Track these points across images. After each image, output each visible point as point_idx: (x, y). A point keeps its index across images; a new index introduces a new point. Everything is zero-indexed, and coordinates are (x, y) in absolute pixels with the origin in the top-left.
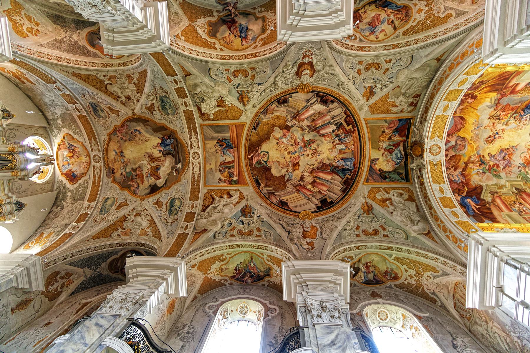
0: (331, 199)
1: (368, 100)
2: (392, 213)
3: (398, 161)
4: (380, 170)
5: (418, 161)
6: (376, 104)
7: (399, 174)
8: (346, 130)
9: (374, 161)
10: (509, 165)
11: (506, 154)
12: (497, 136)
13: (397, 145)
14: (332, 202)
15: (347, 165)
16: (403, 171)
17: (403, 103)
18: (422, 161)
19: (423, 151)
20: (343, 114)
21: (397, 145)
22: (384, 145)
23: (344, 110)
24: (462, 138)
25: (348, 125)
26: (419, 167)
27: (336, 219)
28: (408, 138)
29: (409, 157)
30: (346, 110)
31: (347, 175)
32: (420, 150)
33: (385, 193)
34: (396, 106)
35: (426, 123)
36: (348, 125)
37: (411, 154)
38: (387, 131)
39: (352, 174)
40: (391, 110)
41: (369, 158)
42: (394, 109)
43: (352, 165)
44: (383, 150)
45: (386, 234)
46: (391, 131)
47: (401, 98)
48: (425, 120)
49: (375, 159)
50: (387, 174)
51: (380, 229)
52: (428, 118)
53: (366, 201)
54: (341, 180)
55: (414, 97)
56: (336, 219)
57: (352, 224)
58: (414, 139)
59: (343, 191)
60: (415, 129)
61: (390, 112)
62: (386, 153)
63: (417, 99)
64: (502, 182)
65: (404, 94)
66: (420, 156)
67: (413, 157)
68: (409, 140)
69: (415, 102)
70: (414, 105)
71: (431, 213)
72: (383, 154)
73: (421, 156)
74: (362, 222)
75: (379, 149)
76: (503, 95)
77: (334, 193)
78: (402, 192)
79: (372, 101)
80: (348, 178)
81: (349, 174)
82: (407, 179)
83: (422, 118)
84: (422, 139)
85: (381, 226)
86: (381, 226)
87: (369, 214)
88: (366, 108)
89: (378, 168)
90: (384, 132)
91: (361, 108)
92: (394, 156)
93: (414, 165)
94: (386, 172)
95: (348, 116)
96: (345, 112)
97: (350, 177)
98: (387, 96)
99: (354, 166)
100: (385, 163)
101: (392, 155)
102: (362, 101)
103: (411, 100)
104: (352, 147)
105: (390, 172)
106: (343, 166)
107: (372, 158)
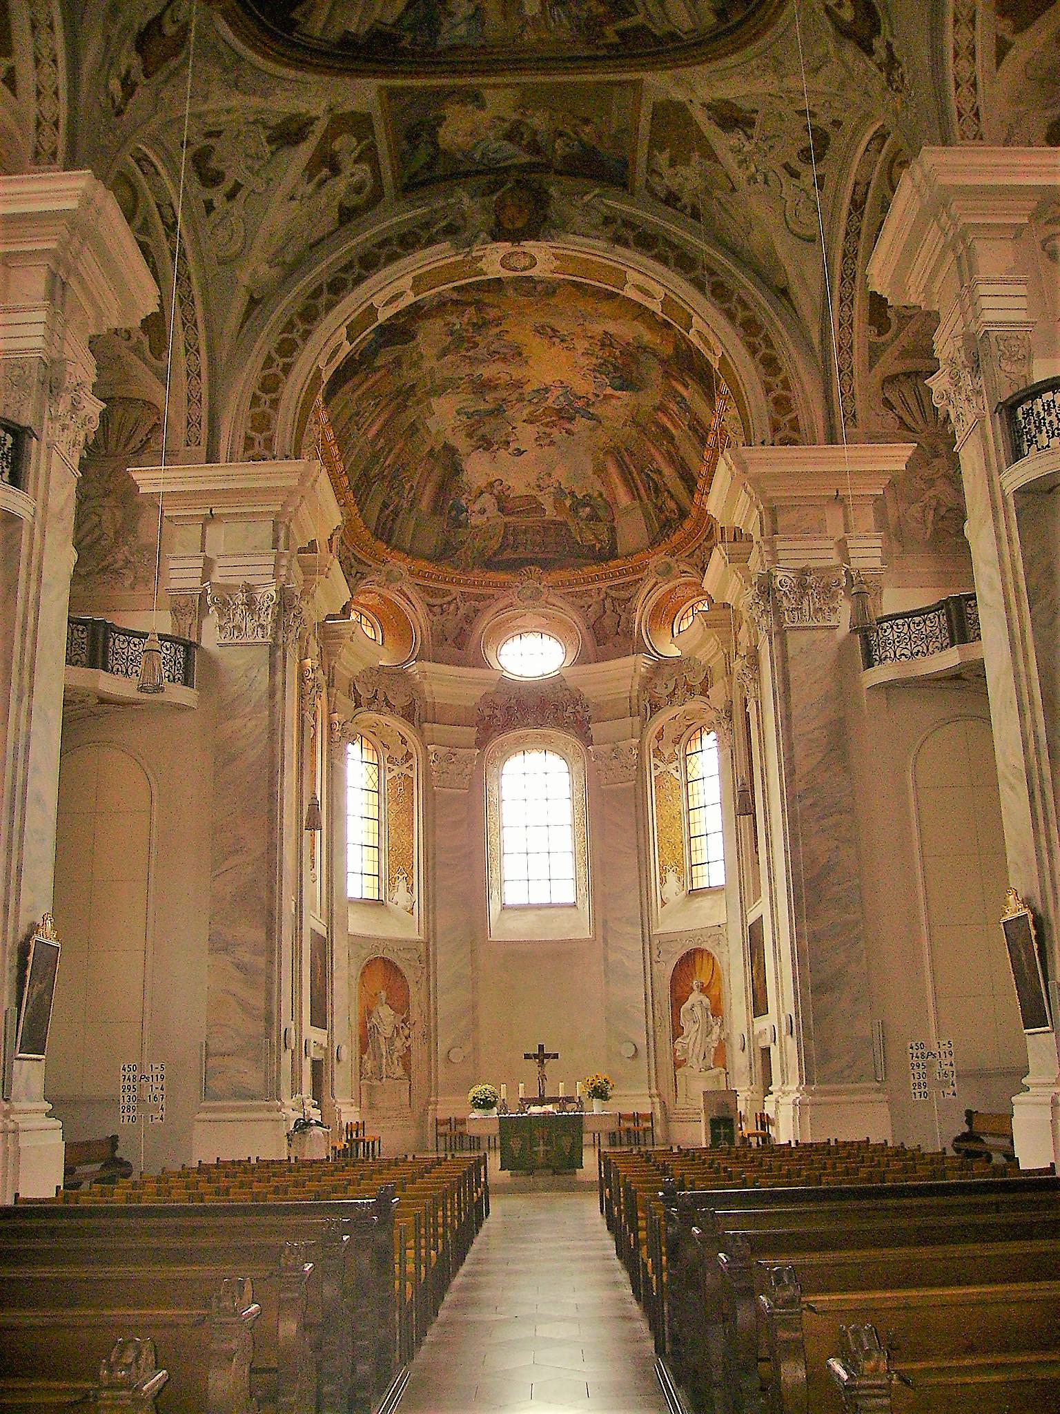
0: (302, 20)
1: (708, 107)
2: (292, 198)
3: (477, 156)
4: (441, 120)
5: (481, 218)
6: (690, 121)
7: (429, 166)
8: (602, 24)
9: (475, 98)
10: (473, 361)
11: (505, 354)
12: (557, 340)
13: (535, 148)
14: (292, 25)
15: (455, 26)
16: (439, 171)
17: (679, 180)
18: (483, 235)
19: (515, 237)
20: (668, 28)
21: (535, 148)
22: (538, 120)
23: (685, 37)
24: (554, 292)
25: (621, 34)
26: (460, 222)
27: (232, 76)
28: (558, 173)
29: (492, 177)
30: (682, 40)
31: (409, 37)
32: (519, 224)
33: (355, 155)
34: (673, 163)
35: (601, 244)
36: (621, 34)
37: (502, 184)
38: (587, 129)
39: (418, 49)
40: (662, 150)
41: (487, 86)
42: (663, 159)
43: (457, 41)
44: (516, 116)
45: (216, 204)
46: (585, 138)
47: (697, 182)
48: (618, 240)
49: (484, 101)
50: (425, 137)
51: (227, 186)
52: (619, 249)
53: (318, 118)
54: (390, 21)
55: (694, 207)
56: (232, 76)
57: (223, 118)
58: (553, 191)
59: (347, 41)
60: (587, 198)
61: (657, 144)
62: (506, 125)
63: (689, 210)
64: (427, 364)
65: (708, 191)
66: (499, 224)
67: (493, 192)
68: (552, 177)
69: (679, 205)
70: (671, 199)
71: (317, 293)
72: (503, 120)
73: (499, 234)
74: (238, 136)
75: (521, 106)
76: (663, 362)
77: (330, 17)
78: (368, 189)
79: (700, 116)
80: (401, 38)
81: (414, 39)
82: (411, 187)
83: (627, 224)
84: (553, 232)
85: (238, 187)
86: (238, 187)
87: (270, 140)
88: (679, 96)
89: (447, 112)
90: (586, 121)
91: (678, 81)
92: (496, 145)
93: (466, 200)
94: (433, 134)
95: (659, 41)
96: (672, 36)
97: (405, 43)
98: (712, 156)
99: (453, 48)
100: (467, 125)
101: (497, 139)
102: (704, 93)
103: (686, 199)
104: (530, 37)
105: (435, 144)
106: (451, 14)
107: (487, 94)
